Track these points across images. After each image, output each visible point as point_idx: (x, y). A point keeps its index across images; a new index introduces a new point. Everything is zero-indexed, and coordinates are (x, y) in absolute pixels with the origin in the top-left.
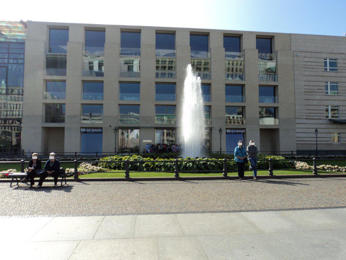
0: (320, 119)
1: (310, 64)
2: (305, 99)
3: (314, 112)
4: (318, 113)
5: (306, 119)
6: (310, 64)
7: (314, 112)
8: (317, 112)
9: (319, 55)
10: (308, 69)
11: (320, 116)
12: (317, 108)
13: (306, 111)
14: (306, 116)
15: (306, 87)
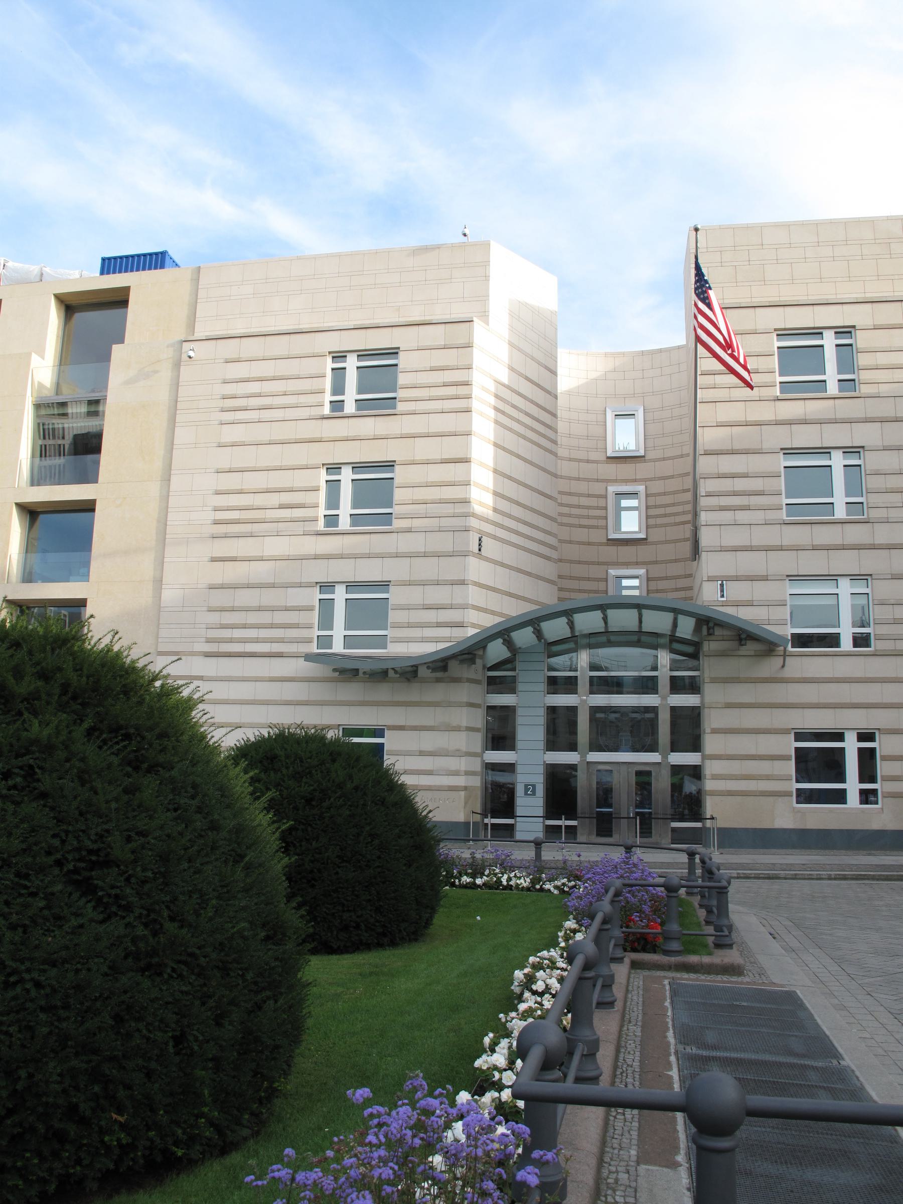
0: (280, 655)
1: (255, 387)
2: (214, 560)
3: (253, 618)
4: (272, 626)
5: (208, 655)
6: (255, 387)
7: (252, 618)
8: (265, 618)
9: (300, 344)
10: (240, 415)
11: (281, 641)
12: (269, 598)
13: (214, 618)
14: (209, 641)
15: (223, 501)
